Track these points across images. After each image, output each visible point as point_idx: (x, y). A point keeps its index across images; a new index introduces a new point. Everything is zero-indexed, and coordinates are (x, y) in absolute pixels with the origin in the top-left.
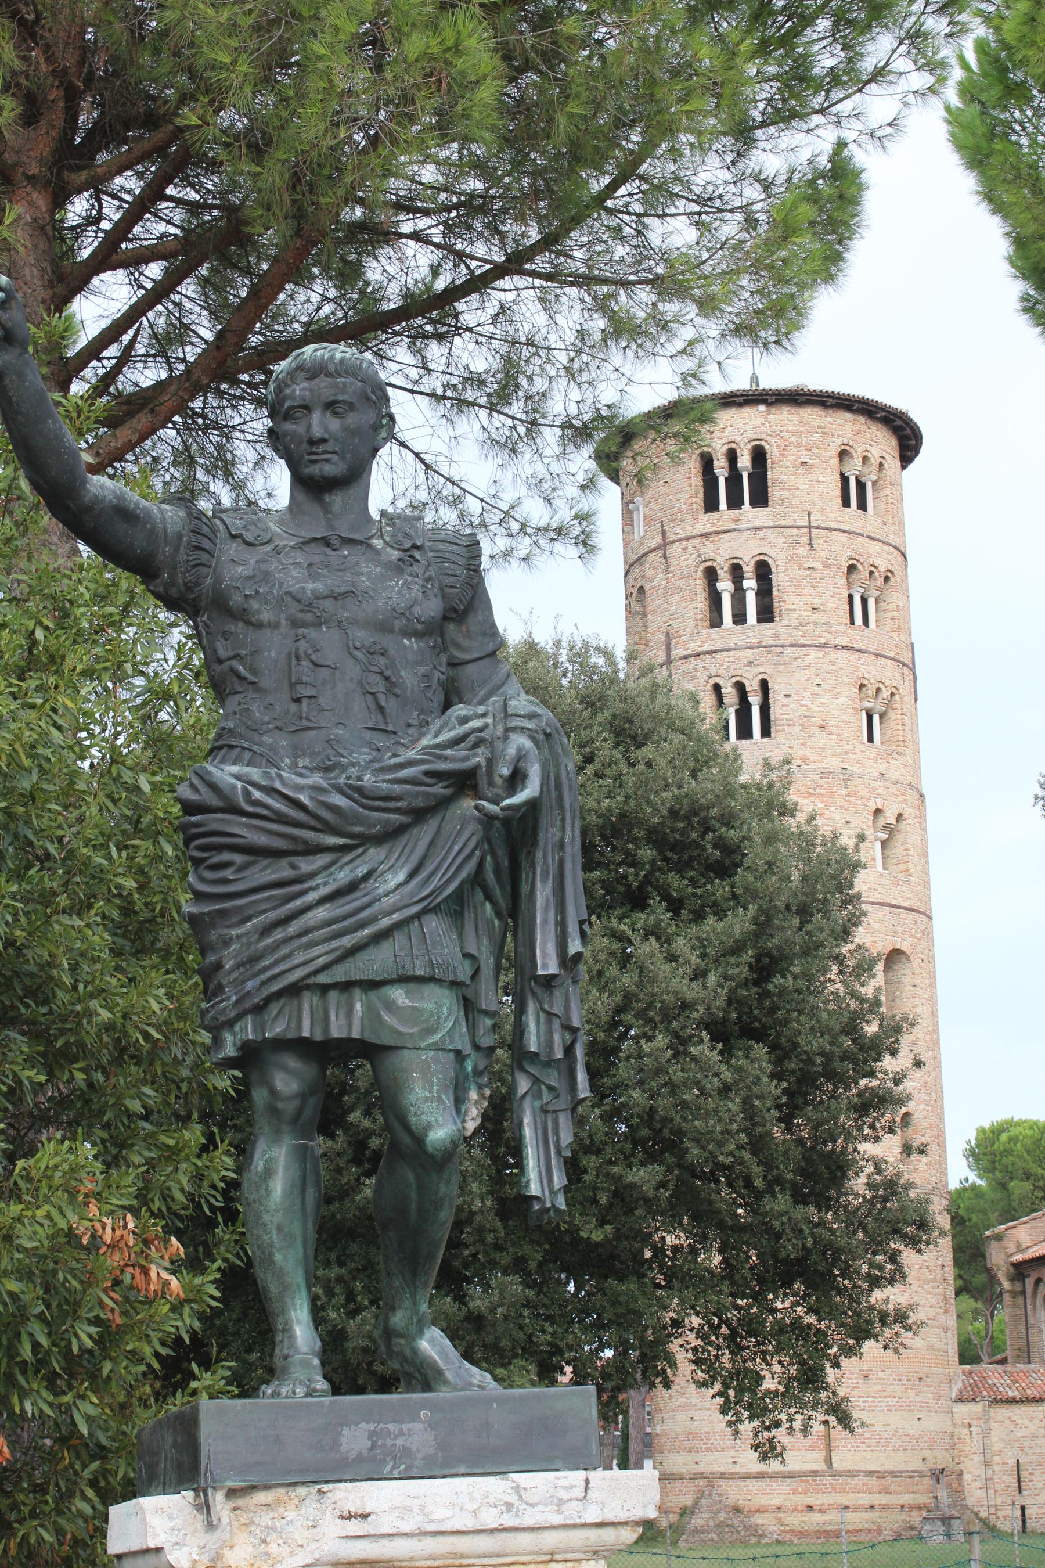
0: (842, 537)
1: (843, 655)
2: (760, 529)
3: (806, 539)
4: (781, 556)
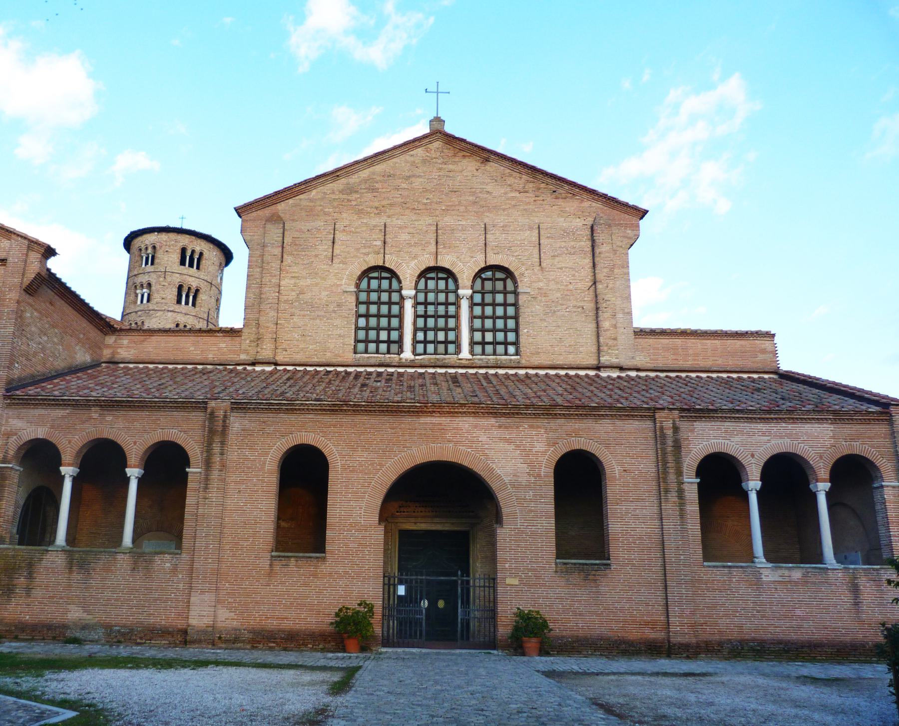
0: (178, 275)
1: (170, 314)
2: (149, 272)
3: (163, 276)
4: (155, 281)
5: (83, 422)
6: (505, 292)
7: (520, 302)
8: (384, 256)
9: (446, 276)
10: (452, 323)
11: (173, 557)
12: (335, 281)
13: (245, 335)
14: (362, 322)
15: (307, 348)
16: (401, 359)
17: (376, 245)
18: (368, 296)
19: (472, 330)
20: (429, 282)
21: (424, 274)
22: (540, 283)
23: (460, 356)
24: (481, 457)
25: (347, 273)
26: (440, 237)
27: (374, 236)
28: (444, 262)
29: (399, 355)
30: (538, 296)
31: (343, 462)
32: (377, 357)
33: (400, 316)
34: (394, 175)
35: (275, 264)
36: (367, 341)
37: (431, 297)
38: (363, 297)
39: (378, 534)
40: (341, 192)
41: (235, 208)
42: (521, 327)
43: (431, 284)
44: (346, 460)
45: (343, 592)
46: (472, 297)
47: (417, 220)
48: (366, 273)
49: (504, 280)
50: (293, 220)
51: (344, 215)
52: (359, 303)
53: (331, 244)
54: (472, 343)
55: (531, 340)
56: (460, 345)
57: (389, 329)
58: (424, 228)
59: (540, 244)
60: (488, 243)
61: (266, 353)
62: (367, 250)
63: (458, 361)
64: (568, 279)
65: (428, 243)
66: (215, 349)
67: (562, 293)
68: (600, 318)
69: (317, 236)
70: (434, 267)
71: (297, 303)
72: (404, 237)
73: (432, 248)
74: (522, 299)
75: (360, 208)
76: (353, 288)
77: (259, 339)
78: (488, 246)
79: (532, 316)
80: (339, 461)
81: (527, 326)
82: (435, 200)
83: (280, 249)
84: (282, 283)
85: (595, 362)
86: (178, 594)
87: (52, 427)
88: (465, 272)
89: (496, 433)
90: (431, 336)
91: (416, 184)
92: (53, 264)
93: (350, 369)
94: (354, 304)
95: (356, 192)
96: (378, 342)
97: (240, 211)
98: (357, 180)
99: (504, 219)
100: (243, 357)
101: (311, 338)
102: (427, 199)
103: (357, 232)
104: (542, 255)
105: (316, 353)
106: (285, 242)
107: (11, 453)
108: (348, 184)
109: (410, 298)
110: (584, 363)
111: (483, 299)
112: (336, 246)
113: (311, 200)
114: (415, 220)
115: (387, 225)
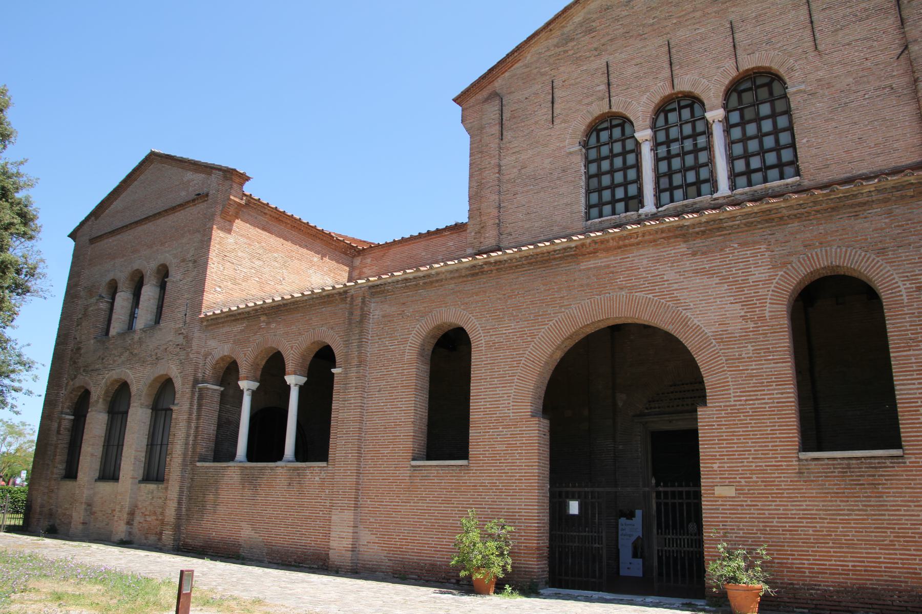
5: (255, 334)
6: (772, 101)
8: (610, 100)
9: (690, 102)
11: (321, 470)
12: (558, 145)
14: (594, 182)
15: (533, 227)
16: (640, 215)
17: (600, 91)
18: (599, 152)
19: (731, 159)
20: (670, 115)
21: (663, 108)
22: (819, 73)
24: (668, 303)
25: (570, 131)
26: (674, 57)
27: (597, 81)
28: (684, 84)
29: (638, 211)
30: (818, 90)
31: (488, 339)
32: (611, 219)
33: (638, 166)
34: (612, 6)
35: (494, 144)
36: (600, 204)
38: (593, 154)
40: (557, 46)
41: (453, 100)
44: (490, 335)
45: (489, 510)
46: (727, 118)
47: (645, 47)
48: (594, 128)
49: (769, 85)
50: (510, 93)
51: (562, 69)
52: (588, 162)
53: (551, 105)
54: (733, 176)
55: (814, 151)
56: (716, 181)
58: (654, 52)
59: (812, 22)
60: (737, 44)
62: (590, 99)
63: (712, 202)
64: (862, 54)
65: (663, 68)
66: (444, 249)
67: (854, 76)
69: (536, 101)
70: (672, 94)
71: (520, 180)
72: (630, 70)
73: (666, 73)
74: (795, 102)
75: (578, 55)
76: (577, 148)
78: (737, 47)
79: (813, 118)
80: (482, 338)
81: (806, 134)
82: (663, 16)
83: (498, 127)
84: (502, 163)
86: (325, 512)
87: (234, 342)
89: (688, 264)
91: (640, 5)
92: (248, 188)
94: (582, 164)
95: (572, 40)
97: (458, 100)
98: (572, 27)
99: (756, 7)
101: (537, 214)
102: (654, 18)
103: (576, 84)
104: (818, 35)
105: (542, 230)
106: (504, 118)
107: (208, 372)
108: (562, 35)
109: (647, 140)
110: (903, 164)
111: (742, 117)
112: (556, 106)
113: (527, 66)
114: (642, 47)
115: (610, 64)
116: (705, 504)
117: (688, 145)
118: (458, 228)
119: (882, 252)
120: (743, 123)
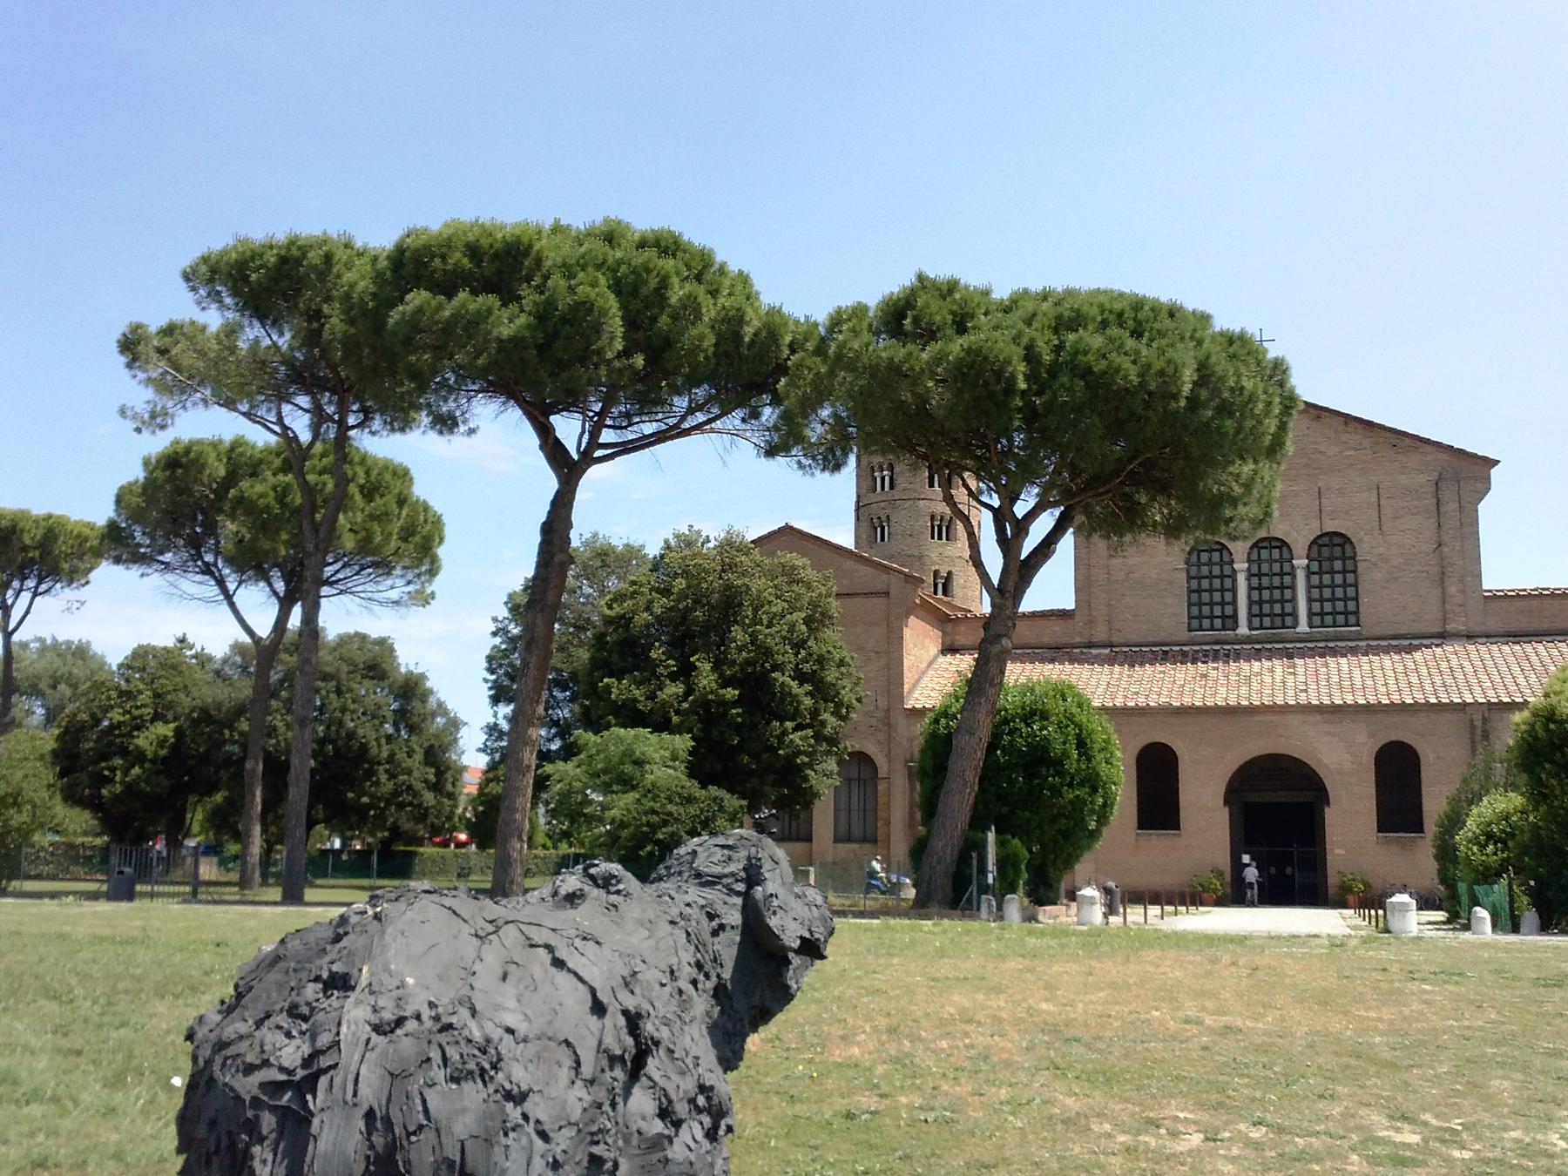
6: (1344, 558)
7: (1360, 570)
9: (1278, 544)
10: (1288, 594)
13: (1077, 617)
14: (1195, 597)
19: (1310, 600)
23: (1298, 630)
33: (1234, 590)
36: (1200, 617)
37: (1265, 568)
39: (1223, 815)
42: (1361, 596)
43: (1265, 554)
49: (1342, 545)
52: (1190, 578)
54: (1311, 614)
57: (1223, 604)
61: (1101, 634)
68: (1446, 584)
74: (1361, 567)
76: (1183, 566)
77: (1091, 623)
85: (1441, 630)
88: (1300, 541)
90: (1266, 608)
93: (1185, 648)
96: (1212, 617)
100: (1078, 639)
111: (1320, 566)
116: (1328, 857)
117: (1276, 581)
118: (1063, 614)
119: (1423, 736)
120: (1320, 573)
